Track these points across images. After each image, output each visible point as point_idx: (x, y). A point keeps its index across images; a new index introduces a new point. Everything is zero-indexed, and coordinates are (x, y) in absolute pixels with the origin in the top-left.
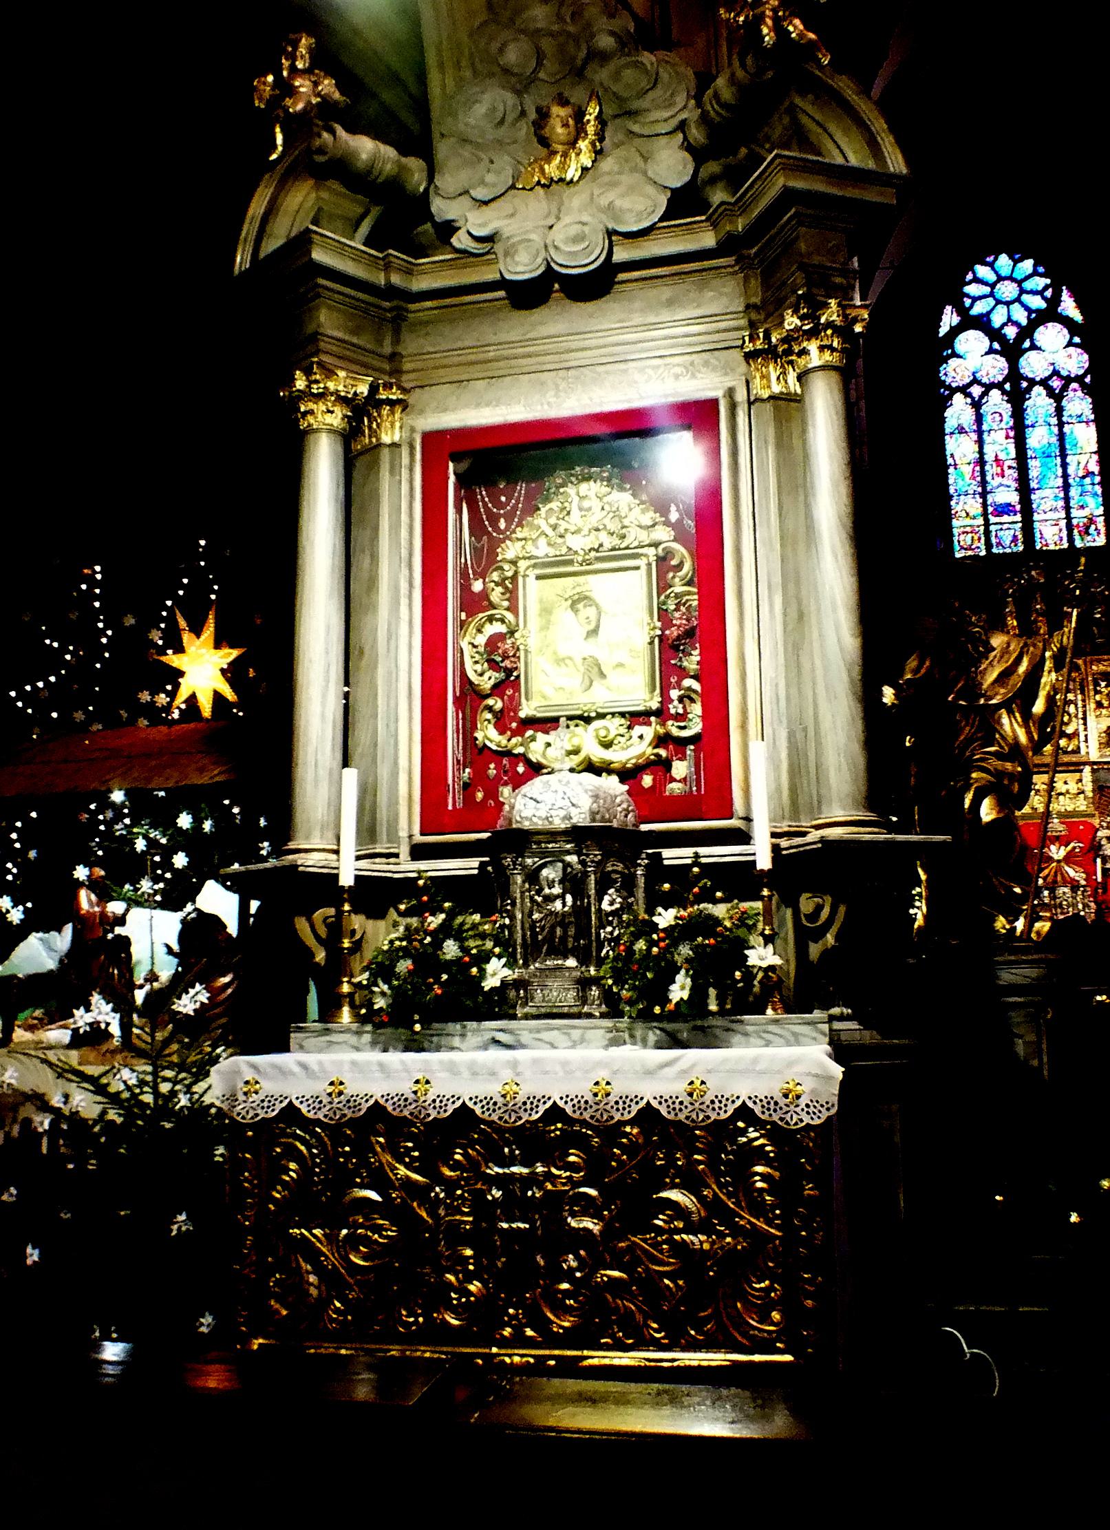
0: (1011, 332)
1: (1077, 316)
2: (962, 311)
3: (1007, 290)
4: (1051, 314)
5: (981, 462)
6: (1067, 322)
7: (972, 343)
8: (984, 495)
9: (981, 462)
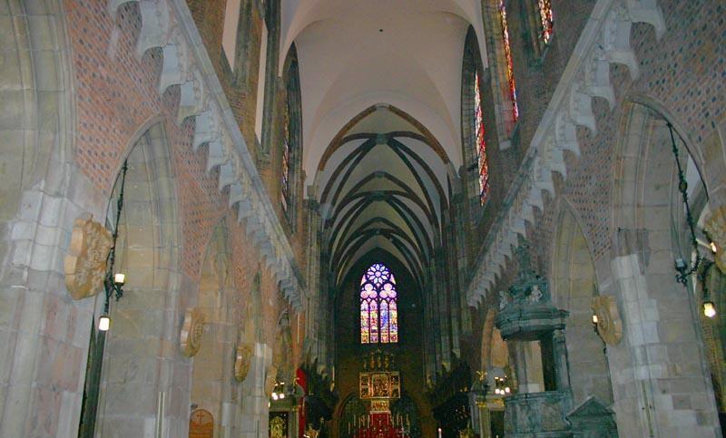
0: (378, 285)
1: (394, 282)
2: (367, 278)
3: (378, 274)
4: (388, 281)
5: (369, 319)
6: (392, 283)
7: (369, 287)
8: (369, 327)
9: (369, 319)
